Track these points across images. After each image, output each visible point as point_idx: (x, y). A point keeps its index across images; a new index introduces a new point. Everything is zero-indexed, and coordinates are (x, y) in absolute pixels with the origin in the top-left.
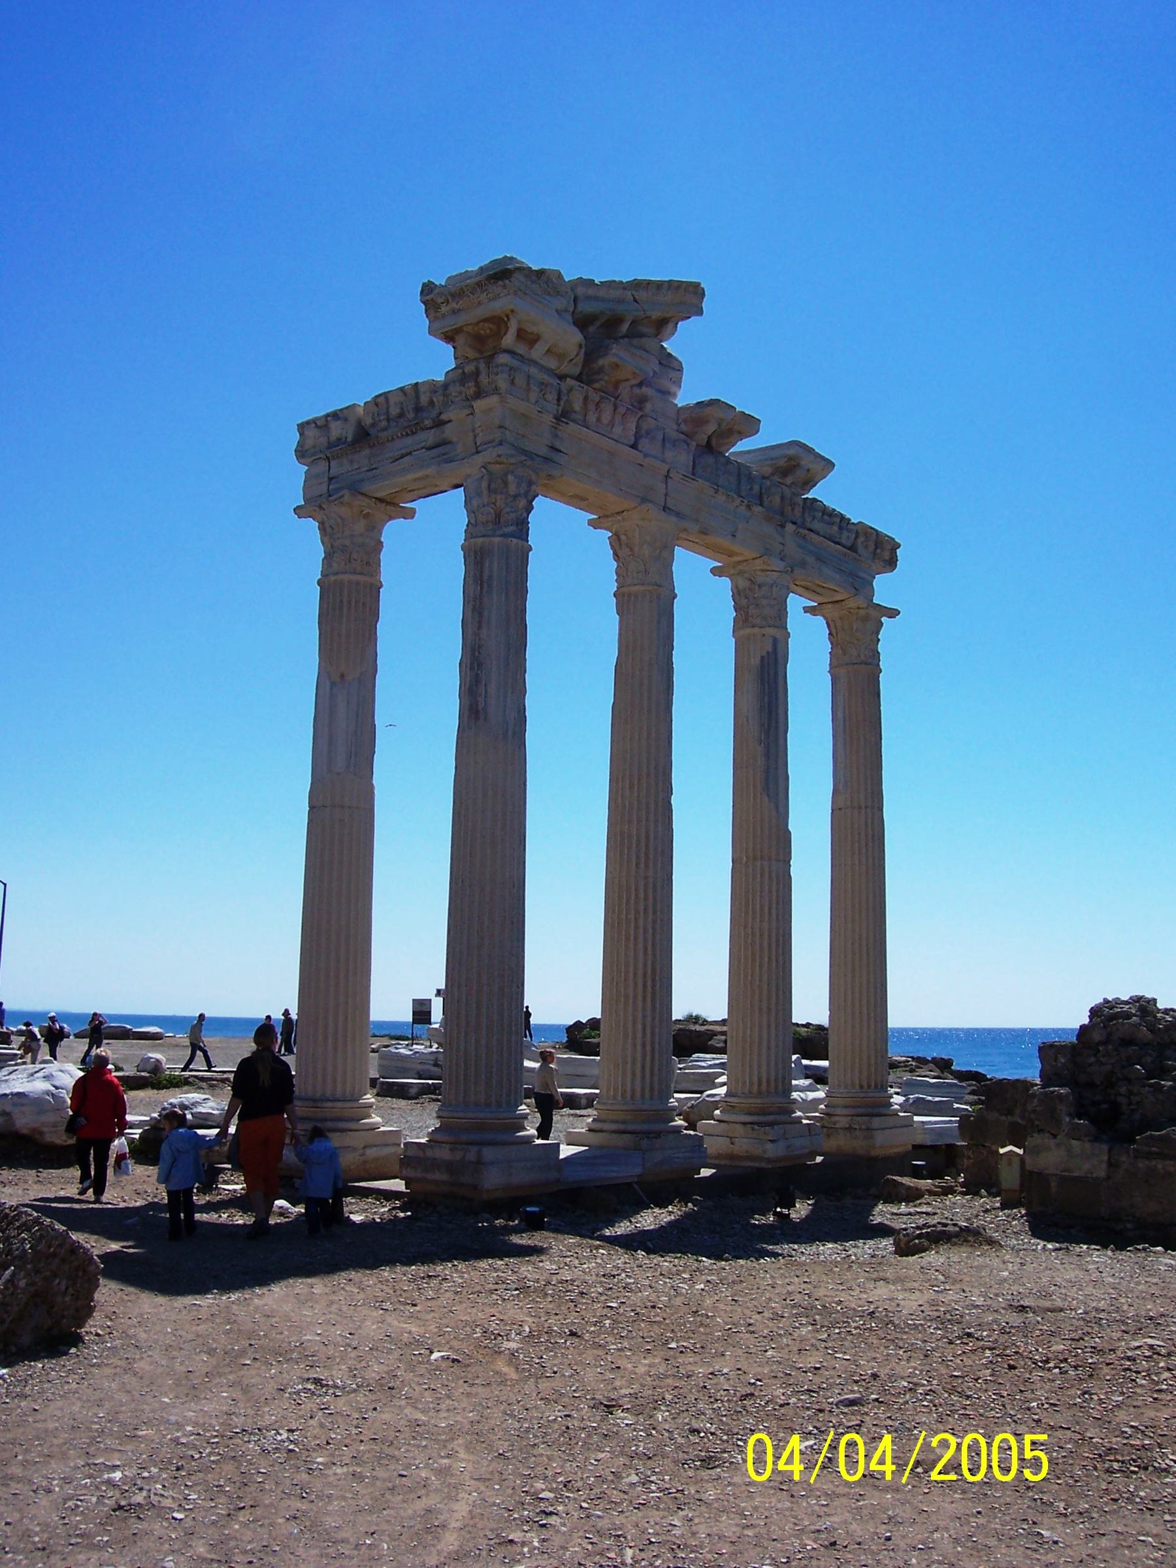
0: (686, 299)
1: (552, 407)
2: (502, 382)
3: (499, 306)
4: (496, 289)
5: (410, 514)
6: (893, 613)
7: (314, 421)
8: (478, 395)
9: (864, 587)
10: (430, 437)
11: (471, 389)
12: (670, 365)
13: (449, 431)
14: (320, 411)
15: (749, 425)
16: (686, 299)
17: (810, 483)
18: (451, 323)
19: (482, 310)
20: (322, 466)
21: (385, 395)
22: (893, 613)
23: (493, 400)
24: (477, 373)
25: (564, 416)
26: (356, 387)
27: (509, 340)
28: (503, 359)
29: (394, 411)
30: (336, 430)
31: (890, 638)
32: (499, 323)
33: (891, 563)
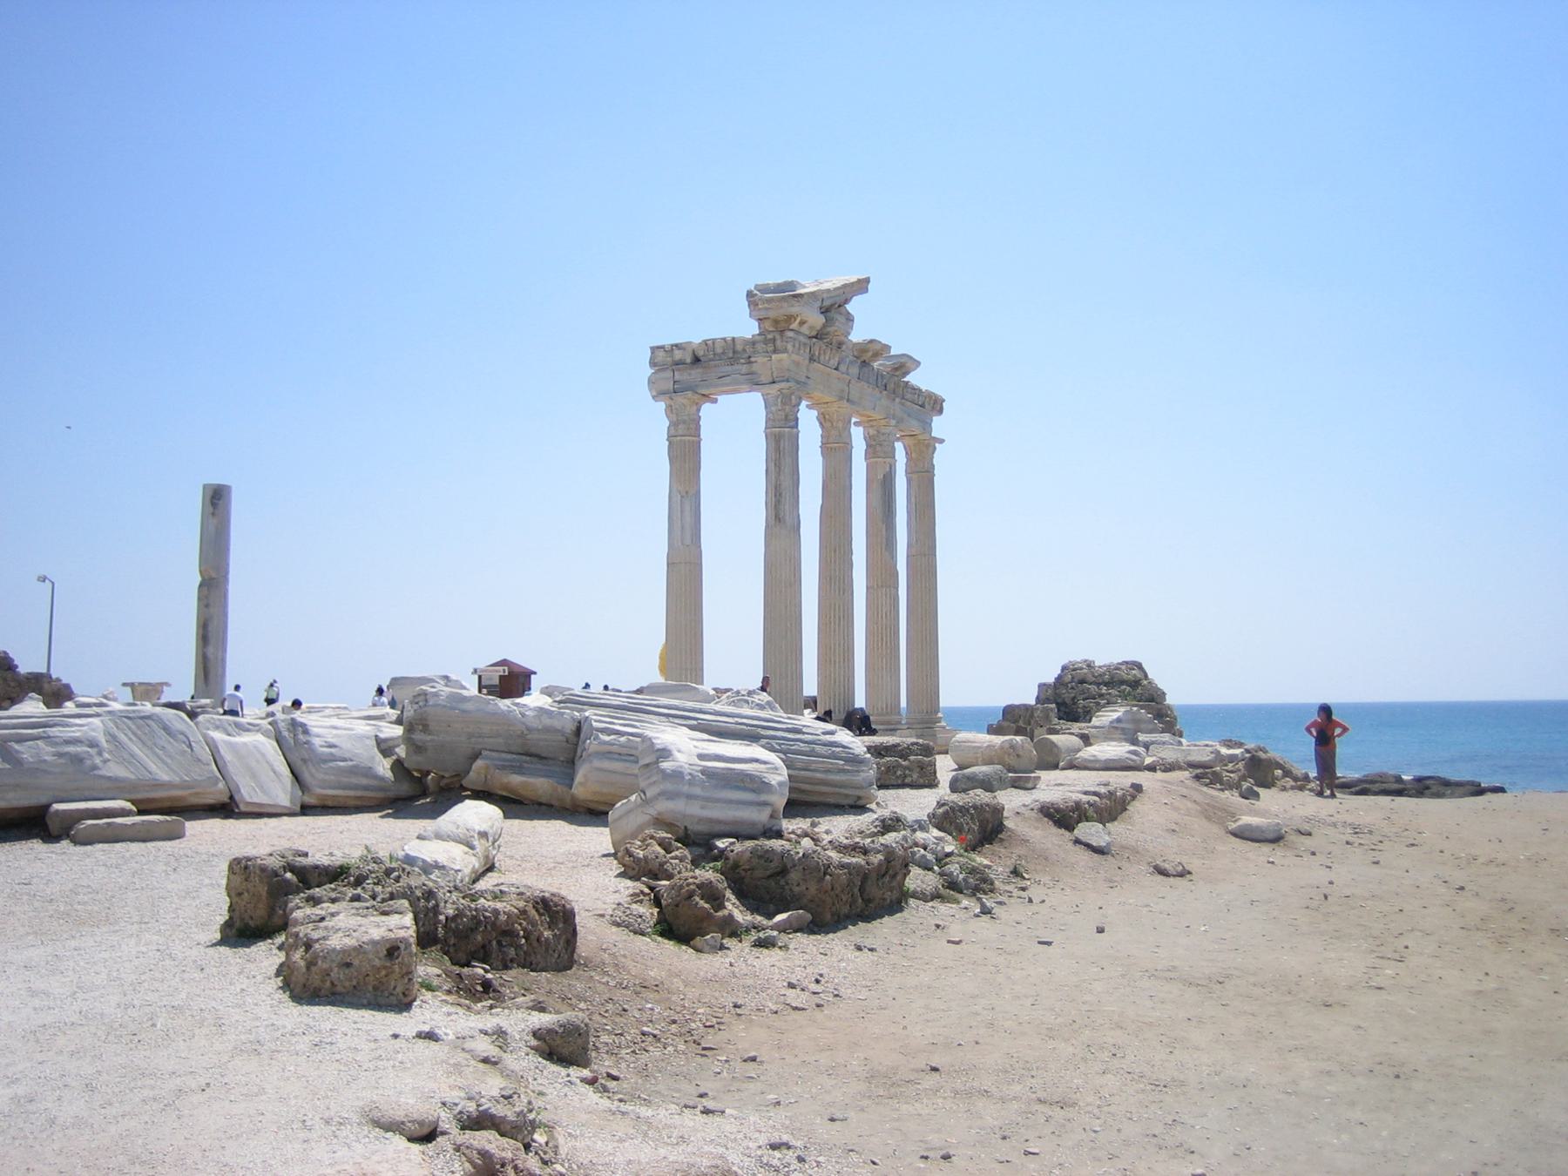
0: (861, 286)
1: (807, 356)
2: (790, 347)
3: (794, 310)
4: (793, 302)
5: (715, 401)
6: (941, 441)
7: (662, 347)
8: (775, 351)
9: (927, 426)
10: (744, 369)
11: (771, 348)
12: (849, 319)
13: (755, 367)
14: (667, 340)
15: (888, 348)
16: (861, 286)
17: (907, 373)
18: (763, 314)
19: (777, 307)
20: (669, 374)
21: (714, 341)
22: (941, 441)
23: (784, 356)
24: (774, 340)
25: (812, 359)
26: (695, 331)
27: (794, 326)
28: (790, 334)
29: (719, 350)
30: (678, 355)
31: (940, 458)
32: (790, 318)
33: (941, 411)
